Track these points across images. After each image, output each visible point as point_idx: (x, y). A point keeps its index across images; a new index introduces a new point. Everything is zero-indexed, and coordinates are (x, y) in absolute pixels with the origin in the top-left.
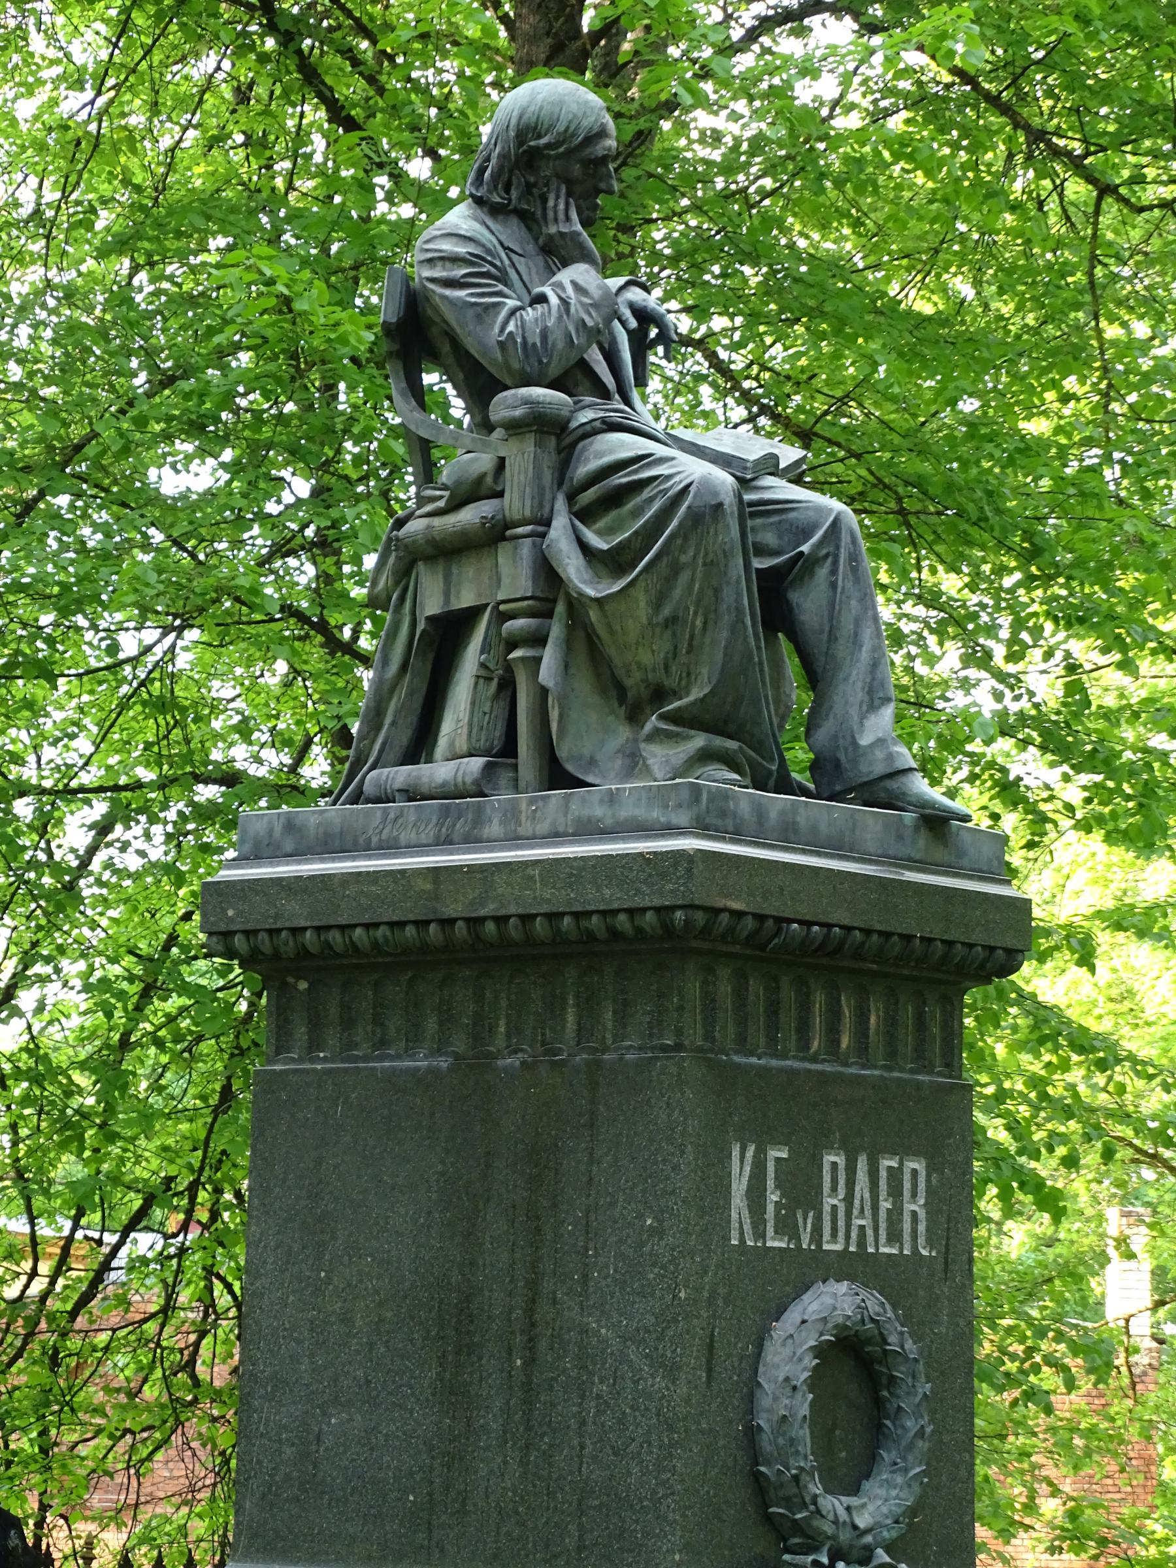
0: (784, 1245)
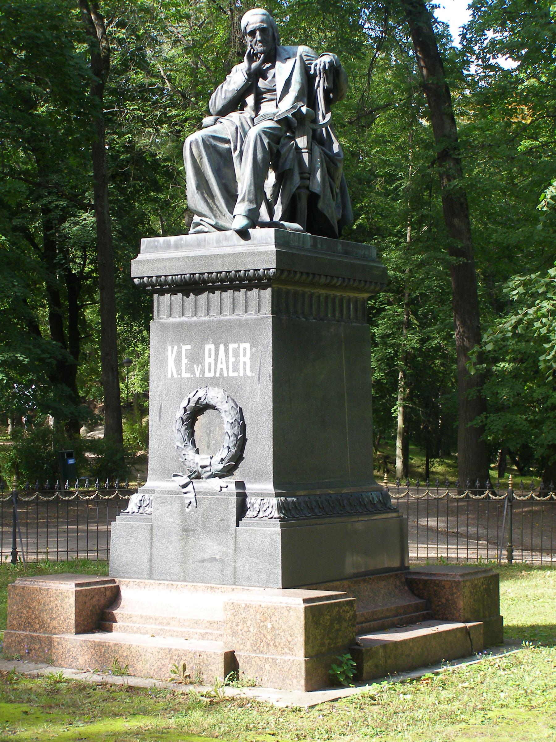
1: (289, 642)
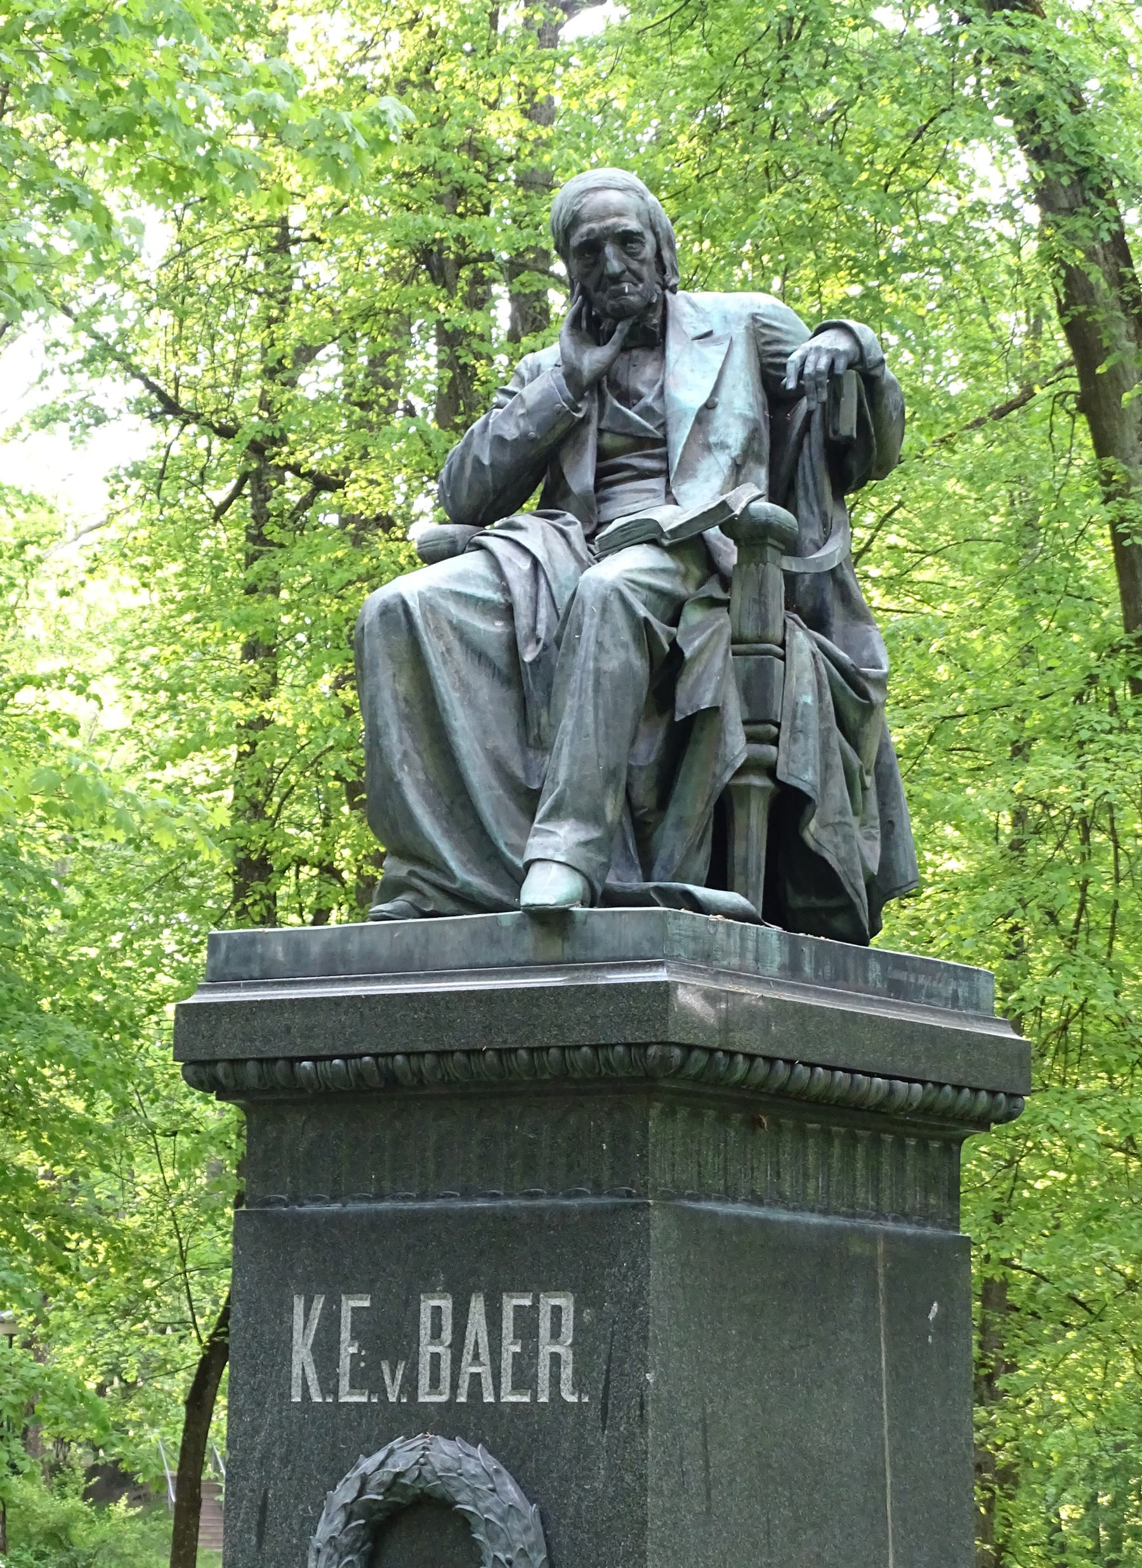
0: (364, 1399)
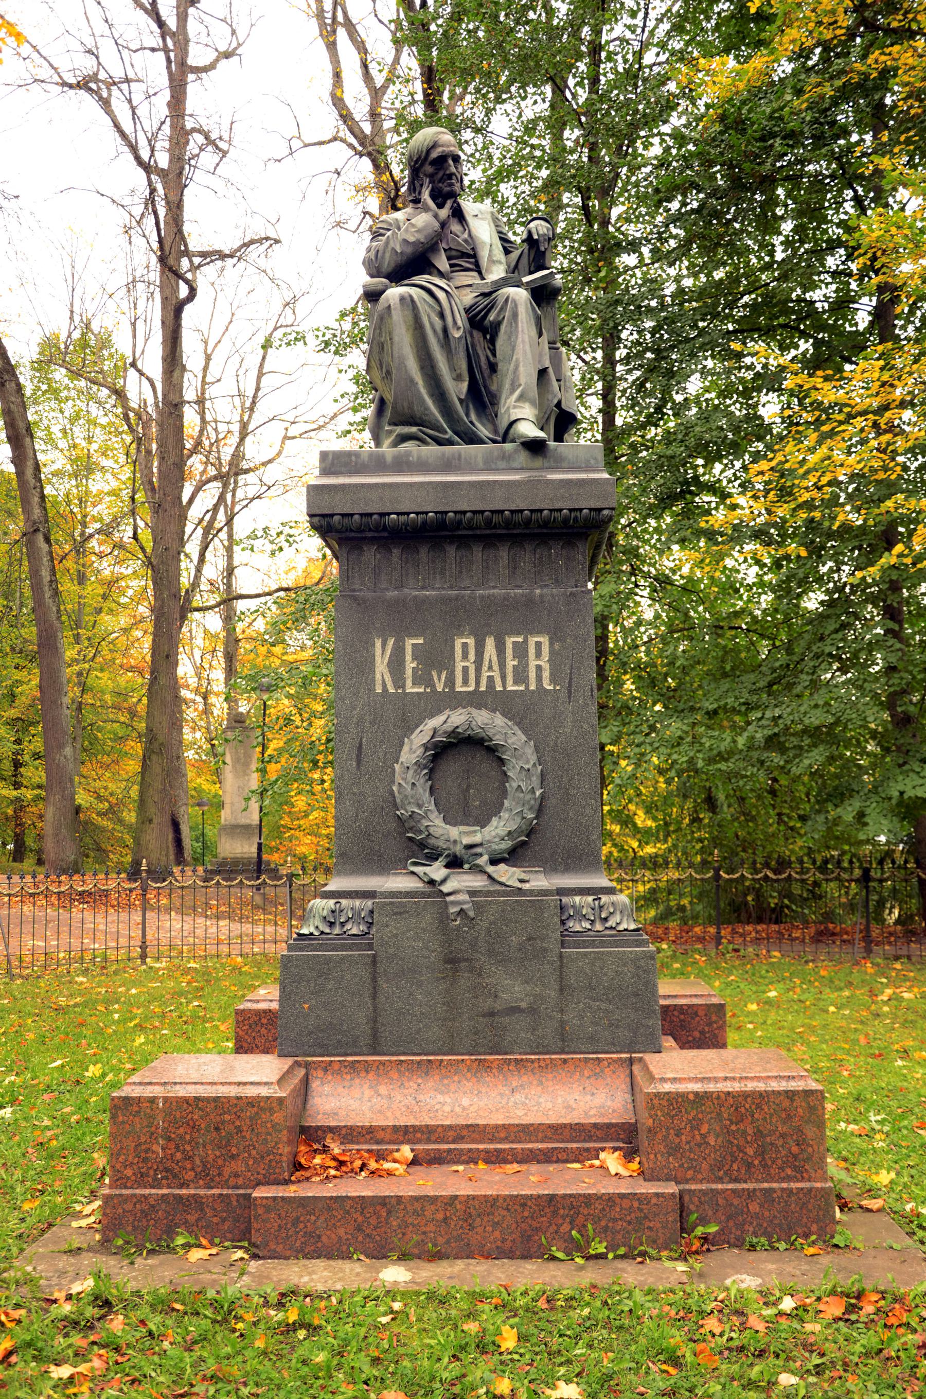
0: (421, 690)
1: (795, 1157)
